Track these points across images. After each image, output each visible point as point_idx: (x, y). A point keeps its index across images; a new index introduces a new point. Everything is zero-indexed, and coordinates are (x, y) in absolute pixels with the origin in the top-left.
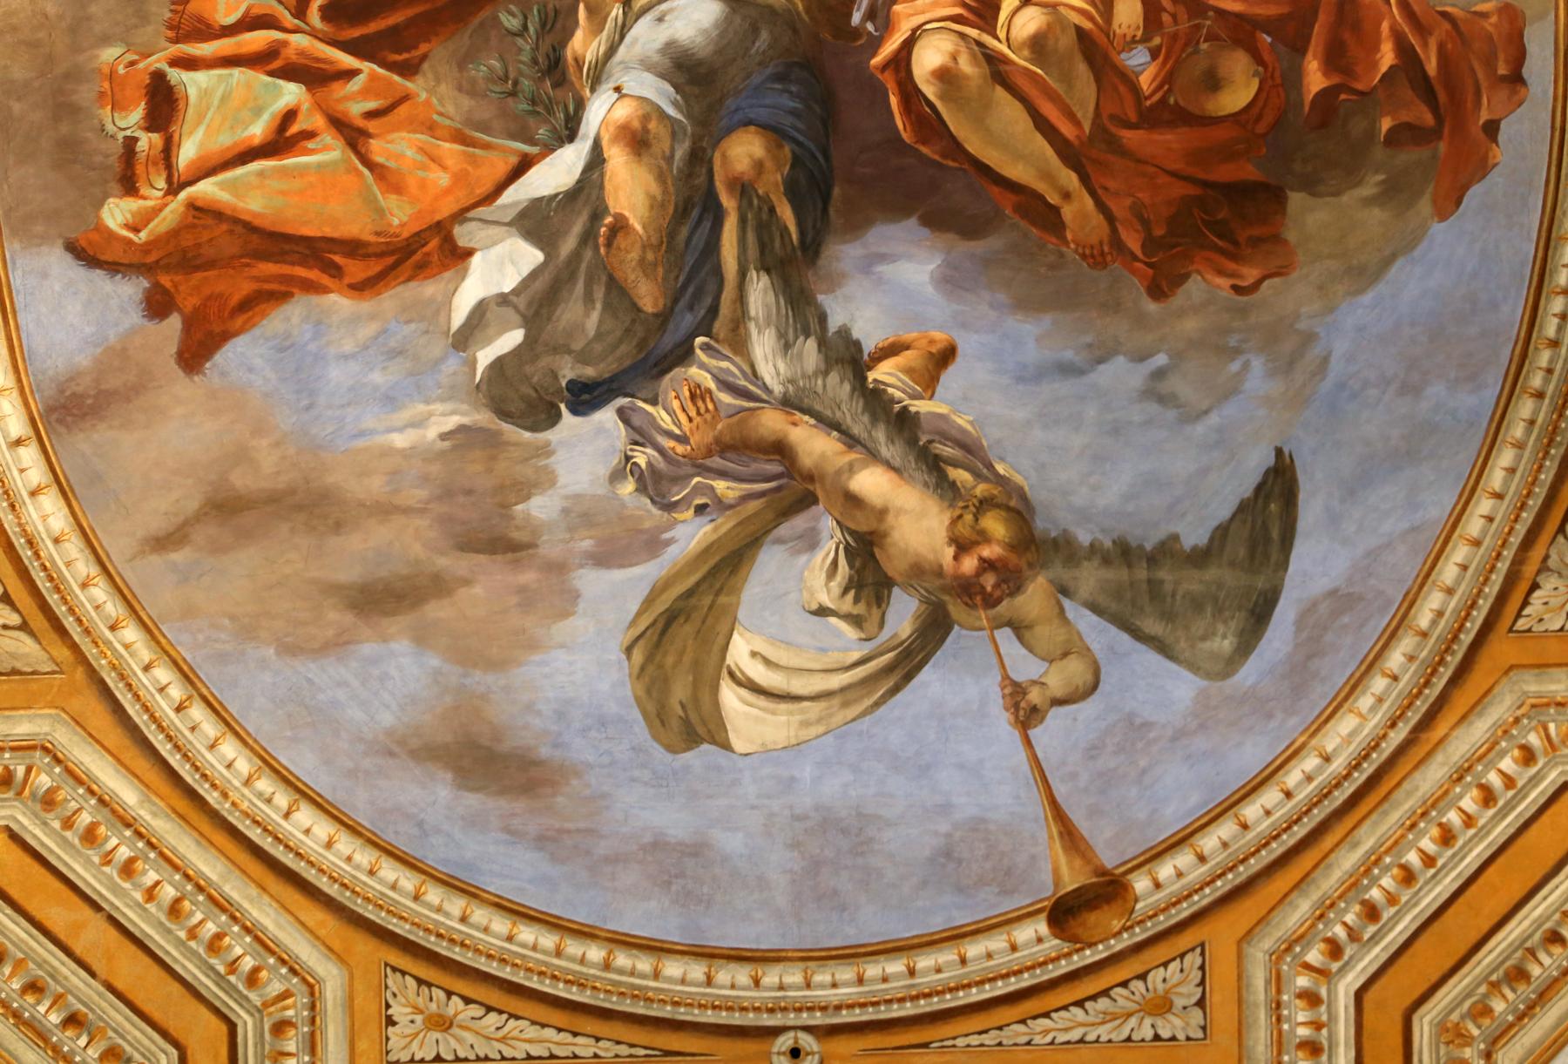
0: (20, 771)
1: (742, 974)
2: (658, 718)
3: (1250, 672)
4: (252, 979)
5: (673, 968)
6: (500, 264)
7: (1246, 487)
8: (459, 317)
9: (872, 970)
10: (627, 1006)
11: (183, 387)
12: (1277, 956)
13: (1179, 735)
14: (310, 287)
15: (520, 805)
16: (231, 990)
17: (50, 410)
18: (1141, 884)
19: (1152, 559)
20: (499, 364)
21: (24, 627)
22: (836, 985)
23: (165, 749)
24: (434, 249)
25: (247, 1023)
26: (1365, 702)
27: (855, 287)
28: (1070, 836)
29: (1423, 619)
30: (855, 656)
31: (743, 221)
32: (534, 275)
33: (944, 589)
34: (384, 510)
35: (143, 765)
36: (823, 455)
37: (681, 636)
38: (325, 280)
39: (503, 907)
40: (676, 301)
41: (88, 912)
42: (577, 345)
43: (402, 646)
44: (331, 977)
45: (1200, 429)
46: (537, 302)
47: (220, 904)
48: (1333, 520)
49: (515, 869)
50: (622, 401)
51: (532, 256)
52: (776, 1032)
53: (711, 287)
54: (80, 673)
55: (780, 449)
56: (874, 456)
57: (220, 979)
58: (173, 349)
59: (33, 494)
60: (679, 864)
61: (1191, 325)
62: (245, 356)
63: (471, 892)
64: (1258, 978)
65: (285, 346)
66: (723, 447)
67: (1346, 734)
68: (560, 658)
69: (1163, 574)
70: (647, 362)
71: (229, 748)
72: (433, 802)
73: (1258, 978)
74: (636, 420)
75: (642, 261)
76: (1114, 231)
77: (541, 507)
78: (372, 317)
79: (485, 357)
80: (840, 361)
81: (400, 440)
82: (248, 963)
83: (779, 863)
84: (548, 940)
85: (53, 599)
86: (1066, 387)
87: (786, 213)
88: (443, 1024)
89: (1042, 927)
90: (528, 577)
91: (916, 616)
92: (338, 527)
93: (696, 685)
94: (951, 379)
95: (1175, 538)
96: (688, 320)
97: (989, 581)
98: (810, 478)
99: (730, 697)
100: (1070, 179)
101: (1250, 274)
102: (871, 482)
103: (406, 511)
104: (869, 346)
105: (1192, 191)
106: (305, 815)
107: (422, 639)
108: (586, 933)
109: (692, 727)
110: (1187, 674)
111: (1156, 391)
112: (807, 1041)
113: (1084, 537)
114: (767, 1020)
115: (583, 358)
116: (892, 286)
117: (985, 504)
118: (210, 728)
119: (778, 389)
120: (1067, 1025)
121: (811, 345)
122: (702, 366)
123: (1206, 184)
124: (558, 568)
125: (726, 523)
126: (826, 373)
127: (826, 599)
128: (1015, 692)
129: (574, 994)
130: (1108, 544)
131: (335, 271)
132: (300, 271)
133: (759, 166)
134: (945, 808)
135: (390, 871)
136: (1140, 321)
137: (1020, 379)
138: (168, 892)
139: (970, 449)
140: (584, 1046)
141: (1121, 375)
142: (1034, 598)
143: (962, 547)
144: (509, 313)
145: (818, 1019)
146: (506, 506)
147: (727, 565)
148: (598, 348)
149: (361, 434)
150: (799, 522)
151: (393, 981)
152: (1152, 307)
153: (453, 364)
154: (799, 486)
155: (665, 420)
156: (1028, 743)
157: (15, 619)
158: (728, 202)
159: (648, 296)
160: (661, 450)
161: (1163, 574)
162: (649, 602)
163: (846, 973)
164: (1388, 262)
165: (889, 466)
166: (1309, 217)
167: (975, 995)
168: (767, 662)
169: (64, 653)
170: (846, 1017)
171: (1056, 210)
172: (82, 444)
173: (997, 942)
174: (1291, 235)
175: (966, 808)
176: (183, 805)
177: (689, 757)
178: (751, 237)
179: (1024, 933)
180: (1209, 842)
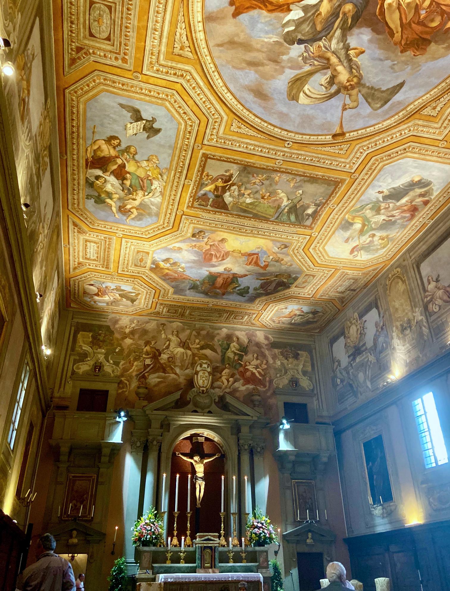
0: (185, 75)
1: (286, 133)
2: (289, 95)
3: (379, 111)
4: (213, 115)
5: (276, 129)
6: (296, 14)
7: (396, 85)
8: (284, 22)
9: (304, 137)
10: (267, 133)
11: (232, 20)
12: (360, 147)
13: (365, 117)
14: (260, 8)
15: (263, 102)
16: (210, 115)
17: (206, 18)
18: (347, 135)
19: (375, 90)
20: (288, 32)
21: (191, 52)
22: (298, 137)
23: (209, 78)
24: (286, 8)
25: (211, 120)
26: (393, 119)
27: (354, 37)
28: (341, 126)
29: (408, 109)
30: (323, 93)
31: (342, 20)
32: (301, 18)
33: (342, 87)
34: (258, 51)
35: (205, 80)
36: (334, 62)
37: (297, 84)
38: (264, 8)
39: (254, 115)
40: (323, 30)
41: (191, 99)
42: (303, 33)
43: (252, 72)
44: (225, 118)
45: (395, 74)
46: (299, 23)
47: (211, 103)
48: (406, 91)
49: (258, 110)
50: (306, 44)
51: (302, 14)
52: (287, 141)
53: (330, 29)
54: (198, 61)
55: (328, 59)
56: (342, 64)
57: (208, 114)
58: (232, 13)
59: (199, 31)
60: (283, 116)
61: (403, 59)
62: (244, 17)
63: (251, 112)
64: (356, 149)
65: (252, 18)
66: (319, 57)
67: (386, 123)
68: (278, 81)
69: (376, 93)
70: (314, 38)
71: (220, 81)
72: (250, 97)
73: (356, 149)
74: (307, 48)
75: (321, 21)
76: (401, 40)
77: (285, 57)
78: (270, 17)
79: (286, 30)
80: (345, 48)
81: (266, 40)
82: (213, 112)
83: (298, 120)
84: (259, 121)
85: (197, 49)
86: (378, 62)
87: (350, 21)
88: (240, 128)
89: (331, 137)
90: (277, 67)
91: (336, 89)
92: (250, 51)
93: (297, 91)
94: (361, 56)
95: (381, 88)
96: (323, 34)
97: (349, 87)
98: (331, 65)
99: (302, 94)
100: (400, 29)
101: (418, 53)
102: (340, 68)
103: (263, 52)
104: (351, 47)
105: (418, 37)
106: (229, 94)
107: (256, 72)
108: (265, 122)
109: (294, 98)
110: (370, 109)
111: (392, 67)
112: (291, 143)
113: (367, 85)
114: (287, 139)
115: (303, 35)
116: (361, 38)
117: (356, 76)
118: (217, 77)
119: (333, 50)
120: (327, 149)
121: (342, 44)
122: (322, 42)
123: (421, 37)
124: (283, 67)
125: (313, 68)
126: (342, 49)
127: (323, 83)
128: (345, 105)
129: (261, 129)
130: (370, 86)
131: (266, 6)
132: (260, 5)
133: (349, 11)
134: (325, 119)
135: (239, 106)
136: (396, 55)
137: (372, 59)
138: (204, 99)
139: (358, 67)
140: (259, 136)
141: (389, 63)
142: (354, 92)
143: (348, 81)
144: (294, 24)
145: (294, 141)
146: (279, 56)
147: (311, 74)
148: (307, 34)
149: (260, 37)
150: (325, 71)
151: (234, 120)
152: (400, 54)
153: (280, 29)
154: (328, 65)
155: (312, 50)
156: (342, 113)
157: (190, 50)
158: (341, 16)
159: (319, 28)
160: (309, 54)
161: (376, 93)
162: (295, 76)
163: (300, 136)
164: (439, 58)
165: (344, 66)
166: (433, 47)
167: (317, 143)
168: (310, 91)
169: (196, 57)
170: (298, 141)
171: (394, 34)
172: (212, 25)
173: (323, 137)
174: (428, 49)
175: (329, 119)
176: (210, 88)
177: (291, 102)
178: (342, 23)
179: (328, 137)
180: (360, 132)
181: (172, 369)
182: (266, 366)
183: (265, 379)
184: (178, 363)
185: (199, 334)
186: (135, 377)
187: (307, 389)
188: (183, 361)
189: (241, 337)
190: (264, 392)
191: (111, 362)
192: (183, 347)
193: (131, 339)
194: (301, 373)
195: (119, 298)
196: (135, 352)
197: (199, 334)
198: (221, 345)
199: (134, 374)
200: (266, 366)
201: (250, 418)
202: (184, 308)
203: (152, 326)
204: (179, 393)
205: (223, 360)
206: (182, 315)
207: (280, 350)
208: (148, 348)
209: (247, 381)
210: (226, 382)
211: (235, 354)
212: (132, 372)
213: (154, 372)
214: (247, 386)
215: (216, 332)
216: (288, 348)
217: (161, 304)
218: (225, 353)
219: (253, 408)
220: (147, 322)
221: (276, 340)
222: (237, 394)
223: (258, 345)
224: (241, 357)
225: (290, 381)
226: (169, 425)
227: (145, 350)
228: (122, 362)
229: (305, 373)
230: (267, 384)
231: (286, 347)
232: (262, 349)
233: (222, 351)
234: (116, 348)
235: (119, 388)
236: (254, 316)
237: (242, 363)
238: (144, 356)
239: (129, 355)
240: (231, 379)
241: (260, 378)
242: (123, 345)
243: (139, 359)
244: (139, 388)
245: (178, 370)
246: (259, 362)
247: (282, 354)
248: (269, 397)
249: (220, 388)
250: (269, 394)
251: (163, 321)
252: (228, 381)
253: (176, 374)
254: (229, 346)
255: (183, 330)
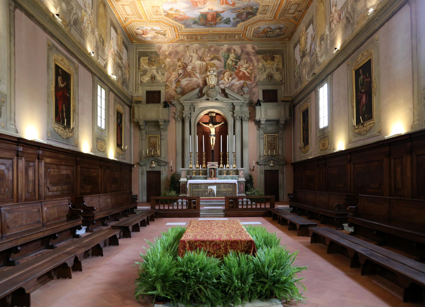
181: (195, 75)
182: (252, 68)
183: (251, 76)
184: (198, 71)
185: (210, 50)
186: (174, 82)
187: (278, 80)
188: (200, 69)
189: (236, 49)
190: (251, 84)
191: (160, 74)
192: (200, 60)
193: (169, 58)
194: (275, 70)
195: (156, 34)
196: (172, 66)
197: (210, 50)
198: (224, 57)
199: (173, 80)
200: (252, 68)
201: (240, 101)
202: (195, 35)
203: (181, 48)
204: (198, 89)
205: (225, 66)
206: (197, 40)
207: (262, 56)
208: (179, 63)
209: (240, 78)
210: (227, 80)
211: (233, 61)
212: (172, 79)
213: (185, 77)
214: (240, 81)
215: (221, 47)
216: (268, 54)
217: (181, 35)
218: (226, 61)
219: (242, 95)
220: (178, 46)
221: (260, 49)
222: (234, 87)
223: (248, 54)
224: (236, 63)
225: (267, 76)
226: (194, 108)
227: (178, 64)
228: (166, 73)
229: (277, 70)
230: (253, 79)
231: (266, 53)
232: (251, 57)
233: (224, 60)
234: (162, 65)
235: (166, 89)
236: (241, 35)
237: (237, 67)
238: (178, 68)
239: (169, 69)
240: (230, 78)
241: (248, 75)
242: (165, 62)
243: (175, 70)
244: (176, 88)
245: (198, 75)
246: (248, 65)
247: (263, 58)
248: (254, 87)
249: (223, 84)
250: (253, 85)
251: (187, 44)
252: (228, 79)
253: (197, 78)
254: (229, 56)
255: (200, 48)
